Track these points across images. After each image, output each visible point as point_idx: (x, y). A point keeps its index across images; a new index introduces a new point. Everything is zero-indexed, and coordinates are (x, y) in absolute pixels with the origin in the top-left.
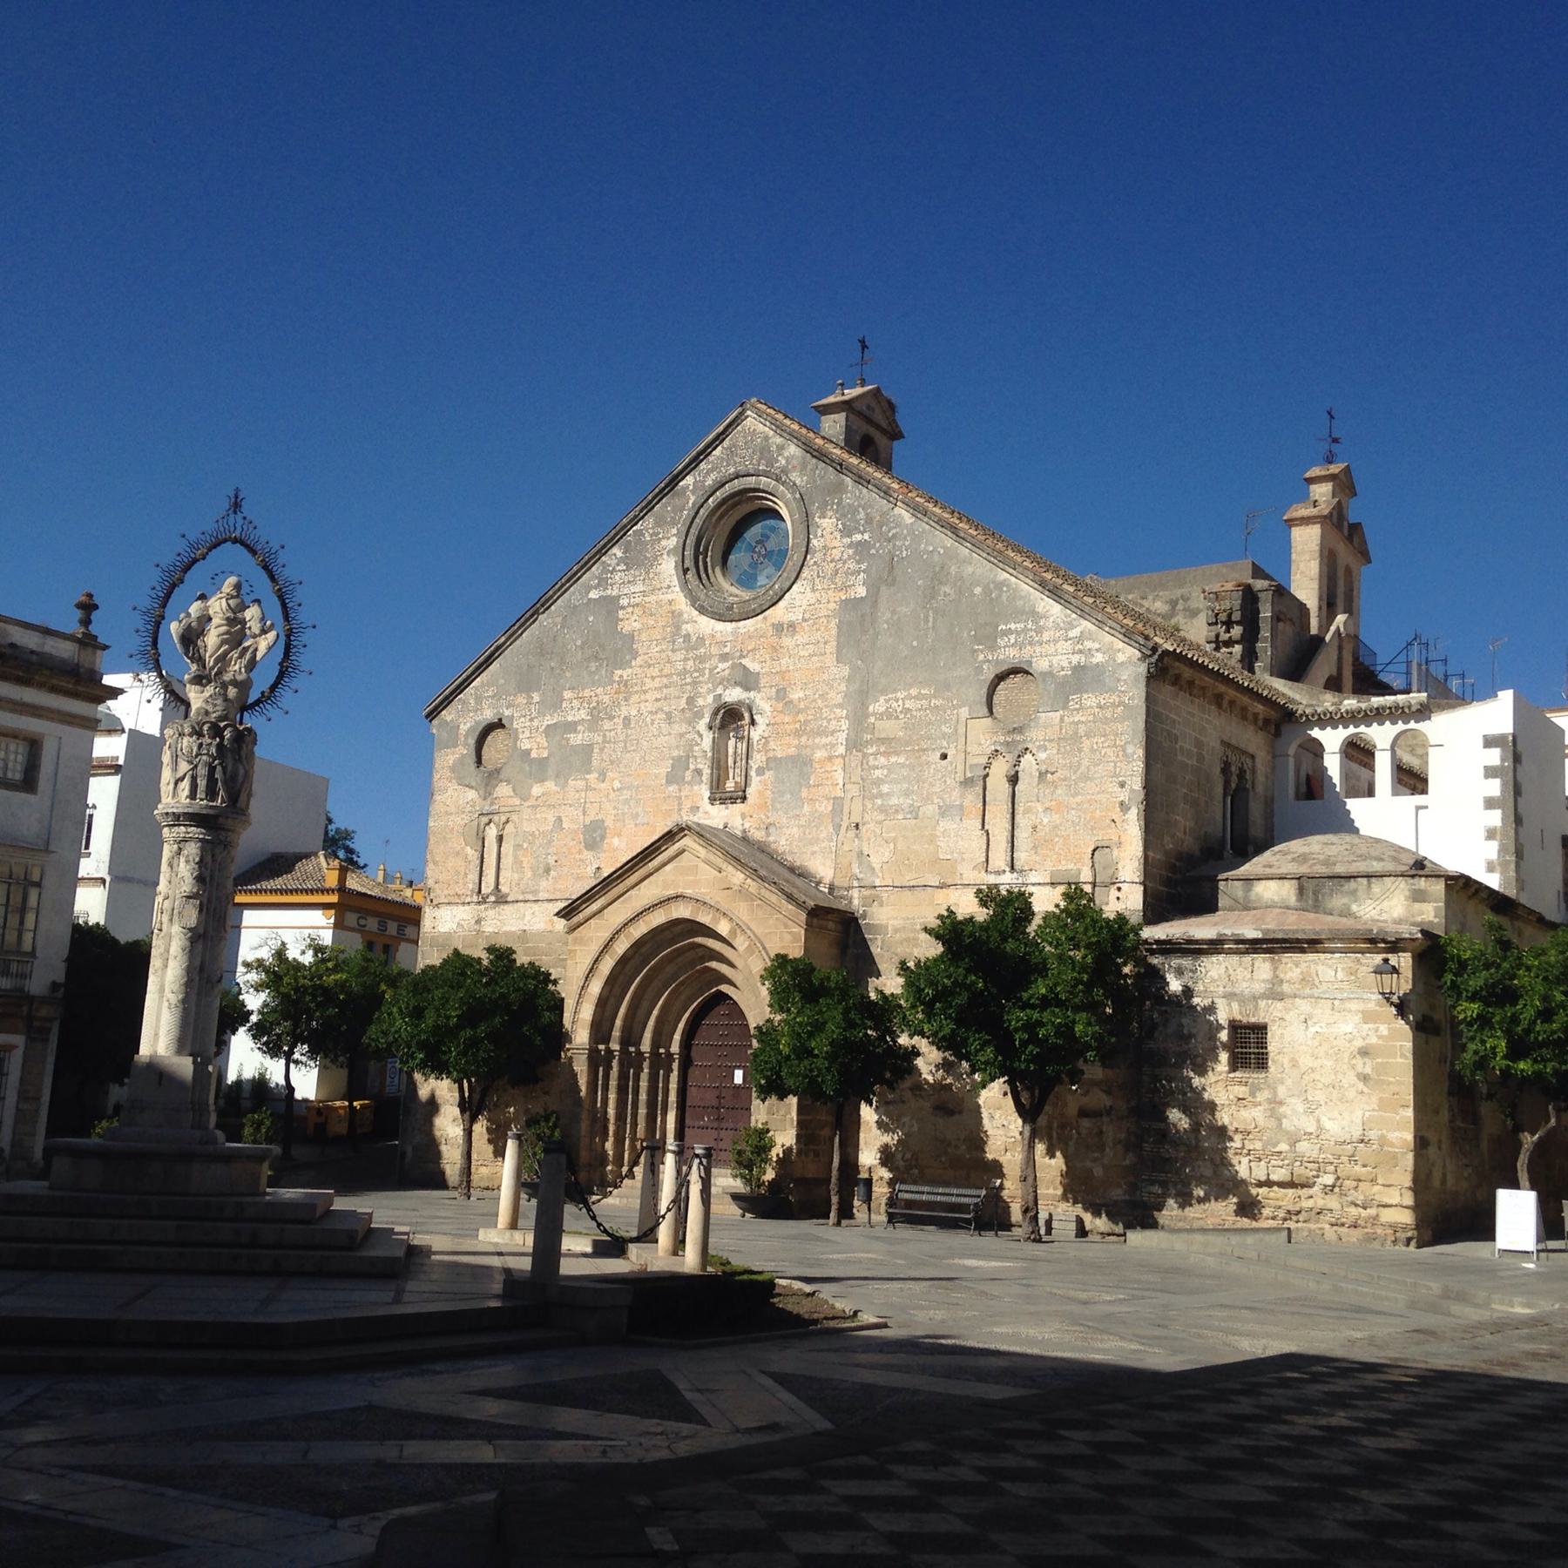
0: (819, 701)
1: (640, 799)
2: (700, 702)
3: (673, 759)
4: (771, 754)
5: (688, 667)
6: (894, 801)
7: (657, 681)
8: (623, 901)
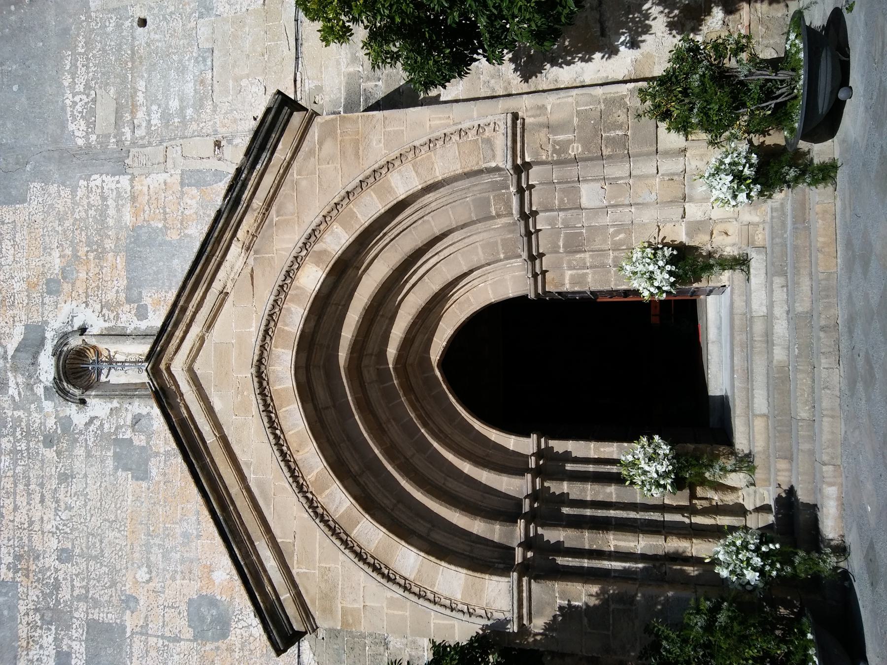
0: (67, 224)
1: (166, 529)
2: (51, 423)
3: (116, 469)
4: (122, 296)
5: (9, 446)
6: (189, 88)
7: (22, 501)
8: (266, 499)
